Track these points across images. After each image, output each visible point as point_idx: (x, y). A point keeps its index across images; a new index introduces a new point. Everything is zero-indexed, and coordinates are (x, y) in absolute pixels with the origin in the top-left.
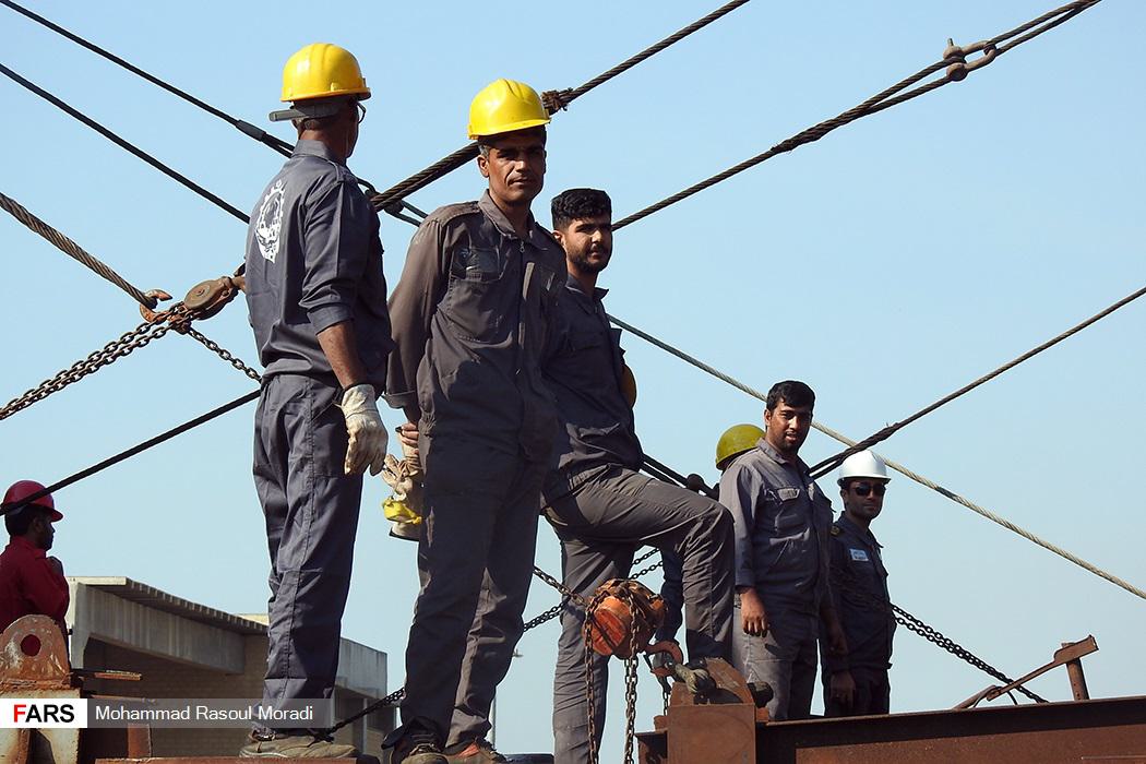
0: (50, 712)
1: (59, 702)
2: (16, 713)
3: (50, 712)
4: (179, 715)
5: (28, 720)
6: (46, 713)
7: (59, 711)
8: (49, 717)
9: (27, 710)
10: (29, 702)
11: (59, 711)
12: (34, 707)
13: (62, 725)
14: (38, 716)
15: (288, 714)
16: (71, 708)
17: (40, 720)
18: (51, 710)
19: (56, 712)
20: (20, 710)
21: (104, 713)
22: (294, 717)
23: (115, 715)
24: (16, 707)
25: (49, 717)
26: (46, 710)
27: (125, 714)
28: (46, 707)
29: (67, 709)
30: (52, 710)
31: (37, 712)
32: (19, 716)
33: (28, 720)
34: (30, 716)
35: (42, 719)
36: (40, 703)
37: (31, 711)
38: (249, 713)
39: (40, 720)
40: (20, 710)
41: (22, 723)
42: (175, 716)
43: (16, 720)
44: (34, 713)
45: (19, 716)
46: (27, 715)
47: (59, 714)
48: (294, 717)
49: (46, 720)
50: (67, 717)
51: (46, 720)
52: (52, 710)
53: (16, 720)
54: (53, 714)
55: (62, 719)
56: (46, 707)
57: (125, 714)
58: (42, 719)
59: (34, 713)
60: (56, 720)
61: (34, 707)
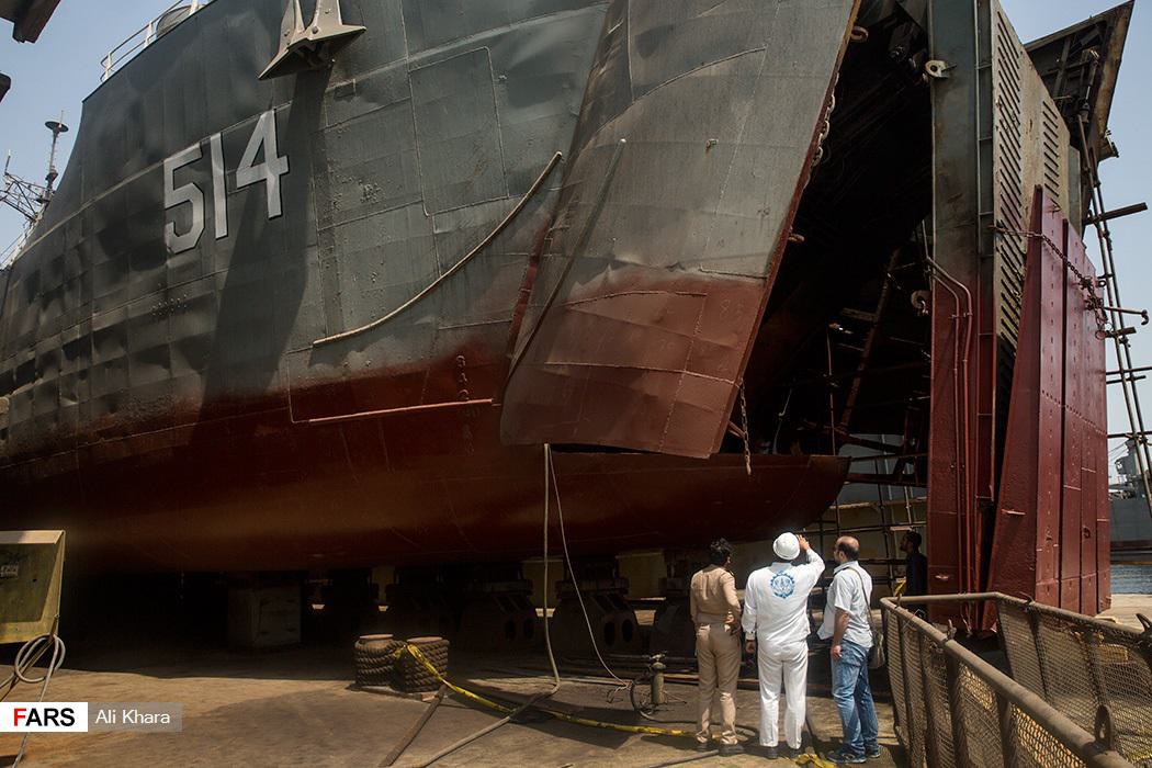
0: (50, 716)
1: (60, 706)
2: (17, 717)
3: (50, 716)
4: (153, 719)
5: (28, 724)
6: (46, 717)
7: (60, 715)
8: (50, 720)
9: (27, 714)
10: (29, 706)
11: (60, 715)
12: (34, 711)
14: (38, 720)
16: (72, 712)
17: (40, 724)
18: (51, 713)
19: (56, 715)
20: (20, 713)
21: (108, 718)
22: (165, 720)
23: (132, 715)
24: (16, 711)
25: (50, 720)
26: (46, 713)
27: (139, 718)
28: (46, 710)
29: (67, 713)
30: (53, 713)
31: (37, 716)
33: (28, 724)
34: (30, 720)
35: (43, 722)
36: (40, 707)
37: (31, 715)
39: (40, 724)
40: (20, 713)
41: (22, 727)
42: (148, 720)
43: (16, 724)
44: (34, 717)
46: (27, 718)
47: (59, 718)
48: (165, 720)
49: (46, 724)
50: (68, 721)
51: (46, 724)
52: (53, 713)
53: (16, 724)
54: (53, 718)
55: (63, 722)
56: (46, 710)
57: (139, 718)
58: (43, 722)
59: (34, 717)
60: (57, 724)
61: (34, 711)
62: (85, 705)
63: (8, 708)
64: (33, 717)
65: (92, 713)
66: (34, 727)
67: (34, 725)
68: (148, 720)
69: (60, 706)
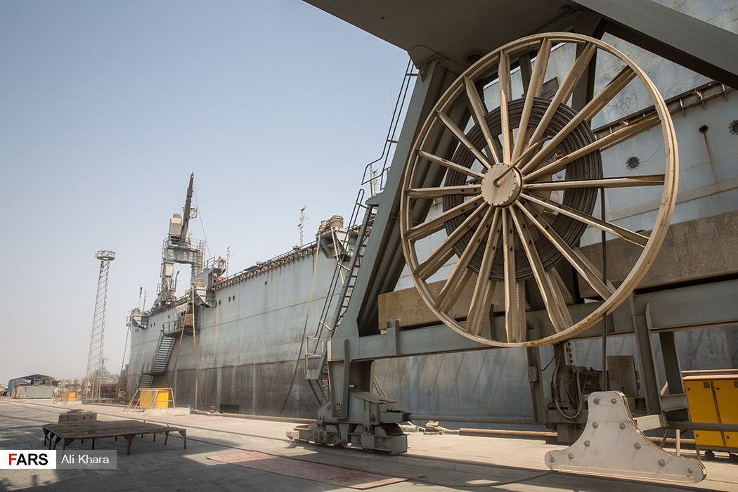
0: (32, 459)
2: (11, 459)
5: (18, 464)
6: (30, 459)
7: (38, 458)
8: (32, 462)
9: (17, 457)
10: (19, 452)
11: (38, 458)
12: (22, 455)
13: (40, 467)
14: (24, 461)
15: (102, 460)
16: (46, 456)
17: (26, 464)
18: (33, 457)
19: (36, 458)
20: (13, 457)
22: (106, 461)
23: (85, 458)
24: (10, 455)
25: (32, 462)
26: (29, 457)
27: (89, 460)
28: (30, 455)
29: (43, 457)
30: (34, 457)
31: (24, 458)
32: (12, 461)
33: (18, 464)
34: (19, 461)
35: (27, 463)
36: (26, 453)
37: (20, 458)
38: (80, 459)
39: (26, 464)
40: (13, 457)
41: (14, 465)
42: (95, 461)
43: (10, 464)
44: (22, 459)
45: (12, 461)
46: (17, 460)
47: (38, 460)
48: (106, 461)
49: (29, 464)
50: (43, 462)
51: (29, 464)
52: (34, 457)
53: (10, 464)
54: (34, 460)
55: (40, 463)
56: (30, 455)
57: (89, 460)
58: (27, 463)
59: (22, 459)
60: (36, 464)
61: (22, 455)
62: (54, 452)
63: (6, 453)
64: (21, 459)
65: (59, 459)
66: (22, 465)
67: (22, 464)
68: (95, 461)
69: (38, 452)
